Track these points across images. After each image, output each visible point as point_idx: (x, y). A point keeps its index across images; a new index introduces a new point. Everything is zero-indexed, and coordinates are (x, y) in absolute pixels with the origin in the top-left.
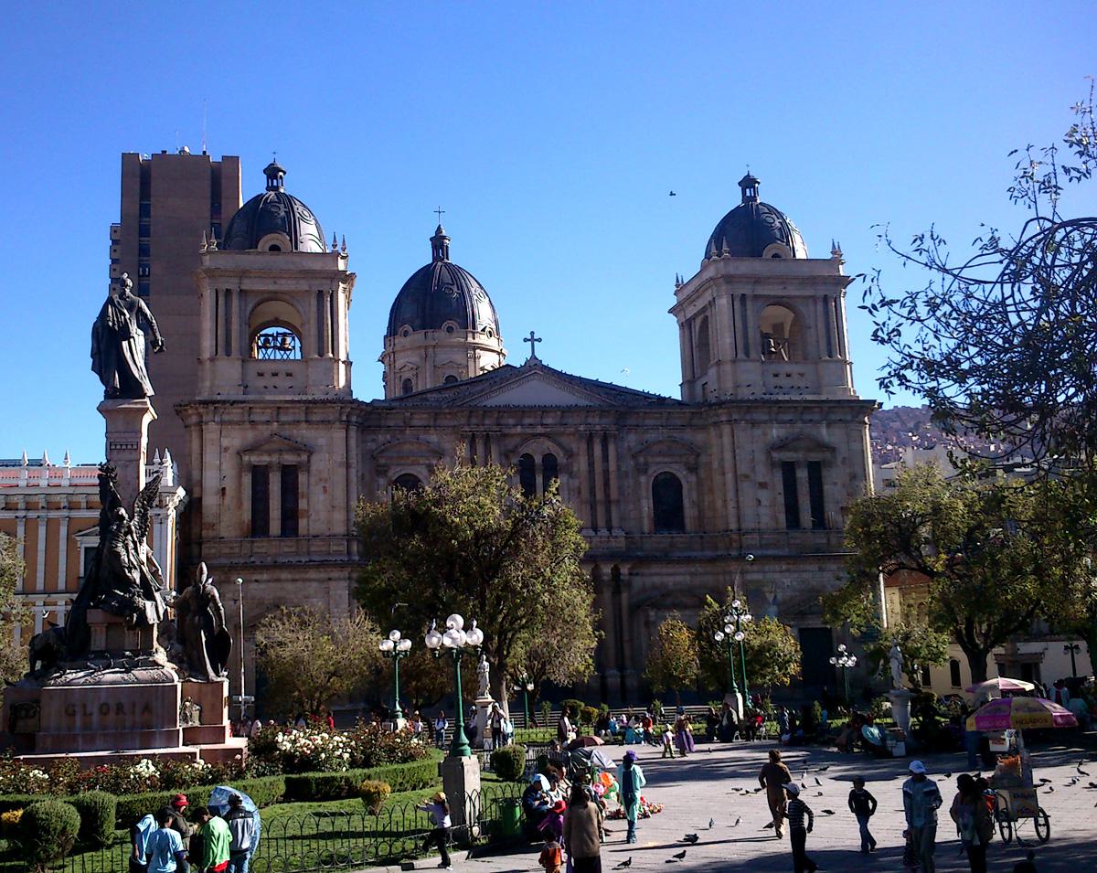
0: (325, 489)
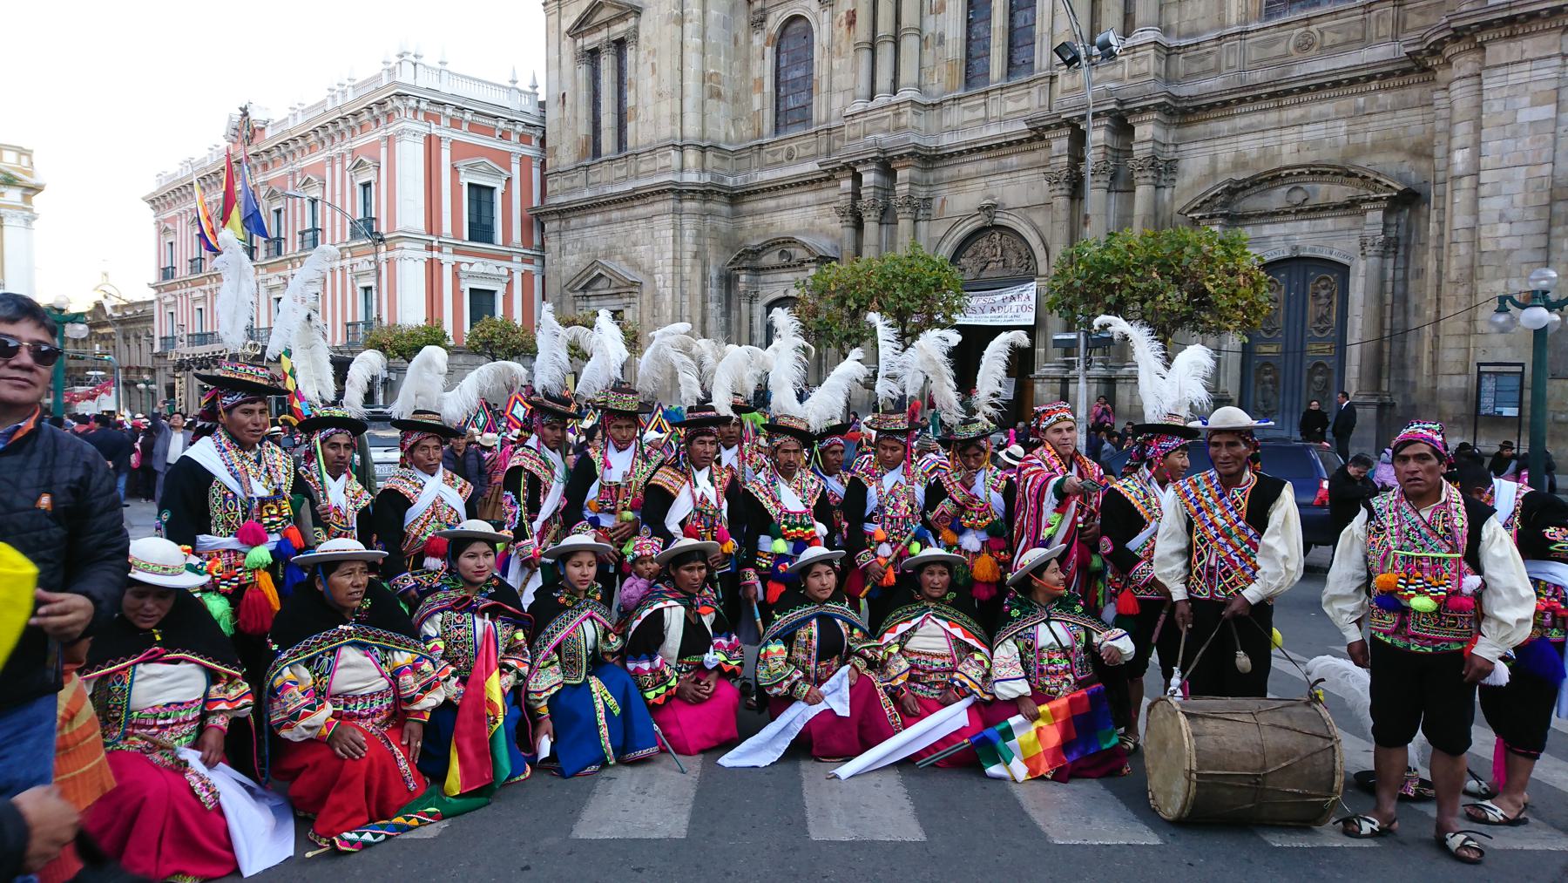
0: (654, 71)
